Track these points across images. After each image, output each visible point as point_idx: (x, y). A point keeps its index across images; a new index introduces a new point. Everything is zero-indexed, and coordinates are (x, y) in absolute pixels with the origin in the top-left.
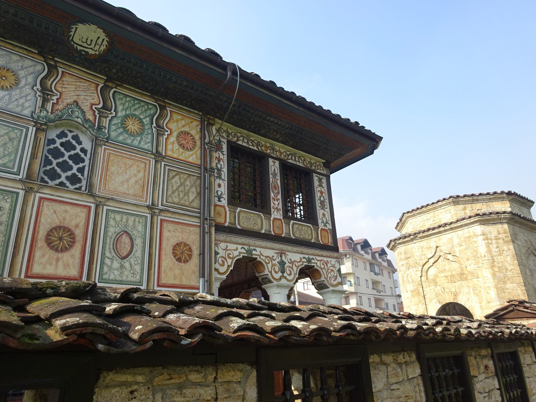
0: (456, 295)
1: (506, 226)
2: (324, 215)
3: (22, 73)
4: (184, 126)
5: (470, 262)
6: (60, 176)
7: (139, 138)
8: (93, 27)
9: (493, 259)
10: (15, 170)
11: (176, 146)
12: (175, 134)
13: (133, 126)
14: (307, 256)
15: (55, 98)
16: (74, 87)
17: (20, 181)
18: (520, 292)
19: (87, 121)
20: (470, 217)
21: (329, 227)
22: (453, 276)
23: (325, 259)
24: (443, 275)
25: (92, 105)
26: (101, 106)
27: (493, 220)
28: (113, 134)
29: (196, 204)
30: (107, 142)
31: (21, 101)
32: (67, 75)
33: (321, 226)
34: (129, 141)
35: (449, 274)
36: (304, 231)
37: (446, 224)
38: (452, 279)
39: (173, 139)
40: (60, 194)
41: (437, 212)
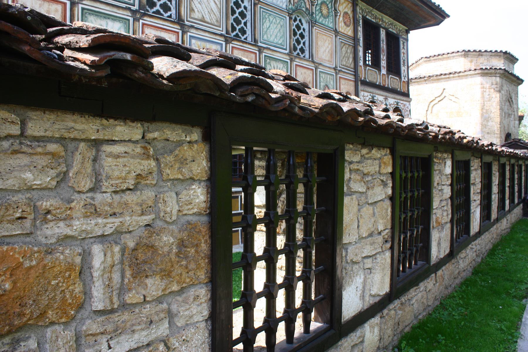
1: (498, 79)
2: (404, 71)
6: (297, 48)
10: (285, 47)
11: (343, 23)
12: (342, 15)
14: (396, 101)
17: (288, 54)
18: (496, 128)
19: (307, 9)
20: (475, 70)
21: (406, 79)
23: (404, 103)
27: (491, 73)
28: (318, 17)
29: (352, 66)
33: (403, 80)
34: (324, 22)
36: (391, 81)
39: (341, 19)
41: (449, 61)
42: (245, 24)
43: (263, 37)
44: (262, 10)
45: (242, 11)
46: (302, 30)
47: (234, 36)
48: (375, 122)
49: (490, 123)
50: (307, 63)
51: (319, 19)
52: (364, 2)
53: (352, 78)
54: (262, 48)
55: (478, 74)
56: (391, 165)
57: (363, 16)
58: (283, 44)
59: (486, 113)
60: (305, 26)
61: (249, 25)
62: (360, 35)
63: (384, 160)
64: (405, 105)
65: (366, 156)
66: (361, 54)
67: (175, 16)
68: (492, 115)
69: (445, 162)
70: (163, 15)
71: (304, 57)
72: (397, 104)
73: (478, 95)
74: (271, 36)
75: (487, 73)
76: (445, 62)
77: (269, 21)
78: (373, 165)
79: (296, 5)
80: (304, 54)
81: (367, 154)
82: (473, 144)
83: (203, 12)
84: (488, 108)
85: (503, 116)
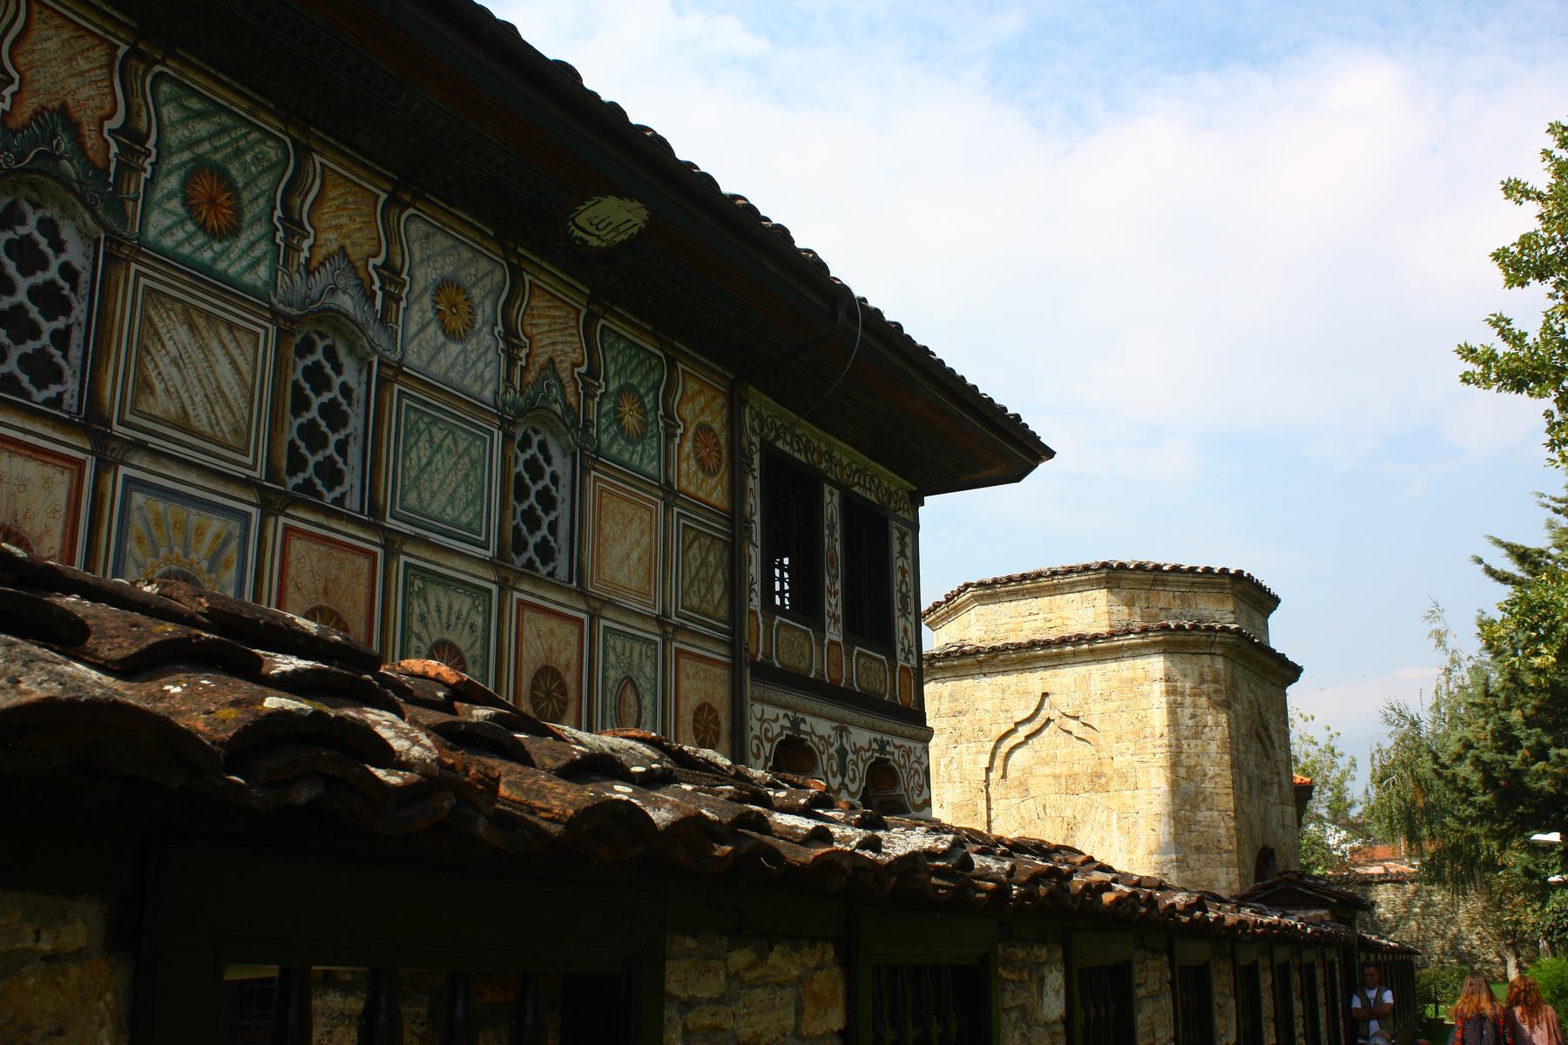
0: (1072, 827)
1: (1220, 664)
2: (905, 630)
3: (477, 293)
4: (703, 410)
5: (1123, 746)
6: (526, 544)
7: (639, 448)
8: (636, 204)
9: (1179, 746)
10: (483, 538)
11: (693, 462)
12: (690, 434)
13: (631, 420)
14: (879, 737)
15: (523, 354)
16: (546, 321)
18: (1222, 831)
19: (568, 408)
20: (1145, 630)
21: (913, 662)
22: (1072, 777)
23: (907, 744)
24: (1047, 770)
25: (574, 365)
26: (583, 369)
27: (1196, 644)
28: (605, 438)
29: (723, 611)
30: (596, 460)
31: (480, 365)
32: (536, 291)
34: (626, 456)
35: (1064, 770)
36: (861, 669)
37: (1080, 638)
38: (1069, 785)
39: (688, 446)
40: (539, 592)
41: (1058, 599)
42: (342, 447)
43: (403, 498)
44: (405, 401)
45: (333, 401)
46: (547, 481)
47: (297, 487)
48: (774, 855)
49: (1203, 815)
50: (561, 599)
51: (611, 444)
52: (768, 395)
53: (720, 653)
54: (398, 539)
55: (1155, 643)
56: (841, 1001)
57: (762, 441)
58: (475, 525)
59: (1189, 778)
60: (560, 465)
61: (354, 451)
62: (754, 503)
63: (816, 987)
64: (909, 752)
65: (747, 976)
66: (755, 570)
67: (75, 402)
68: (1208, 786)
69: (1042, 979)
70: (28, 396)
71: (551, 574)
72: (882, 749)
73: (1158, 718)
74: (433, 495)
75: (1183, 644)
76: (1043, 602)
77: (431, 441)
78: (773, 1008)
79: (529, 391)
80: (552, 565)
81: (751, 967)
82: (1135, 910)
83: (185, 396)
84: (1192, 762)
85: (1245, 787)
